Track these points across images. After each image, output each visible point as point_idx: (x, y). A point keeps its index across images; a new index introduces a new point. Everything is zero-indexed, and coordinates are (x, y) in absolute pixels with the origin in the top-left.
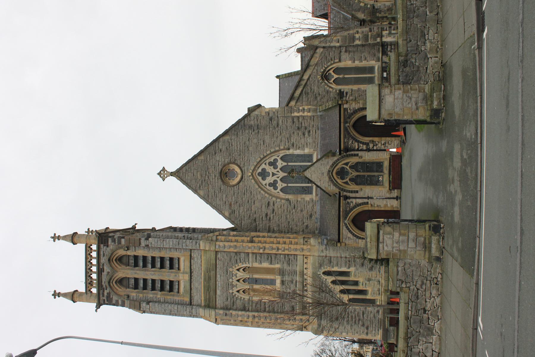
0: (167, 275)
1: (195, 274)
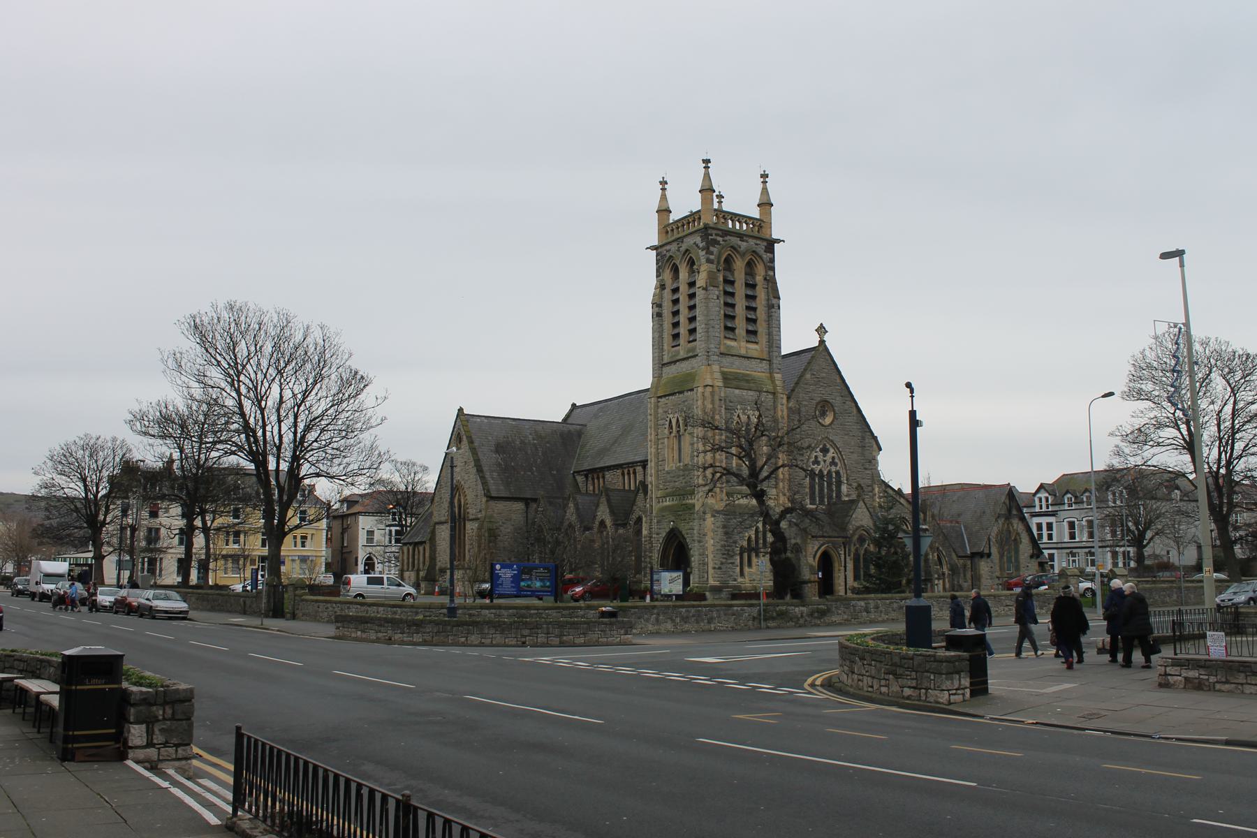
0: (741, 325)
1: (746, 362)
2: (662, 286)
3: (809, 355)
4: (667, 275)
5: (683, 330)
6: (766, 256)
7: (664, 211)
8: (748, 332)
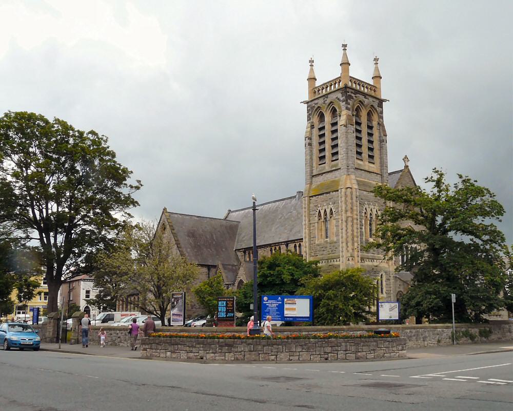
0: (365, 150)
1: (369, 175)
2: (312, 127)
3: (398, 175)
4: (316, 119)
5: (328, 153)
6: (379, 109)
7: (312, 79)
8: (370, 156)
